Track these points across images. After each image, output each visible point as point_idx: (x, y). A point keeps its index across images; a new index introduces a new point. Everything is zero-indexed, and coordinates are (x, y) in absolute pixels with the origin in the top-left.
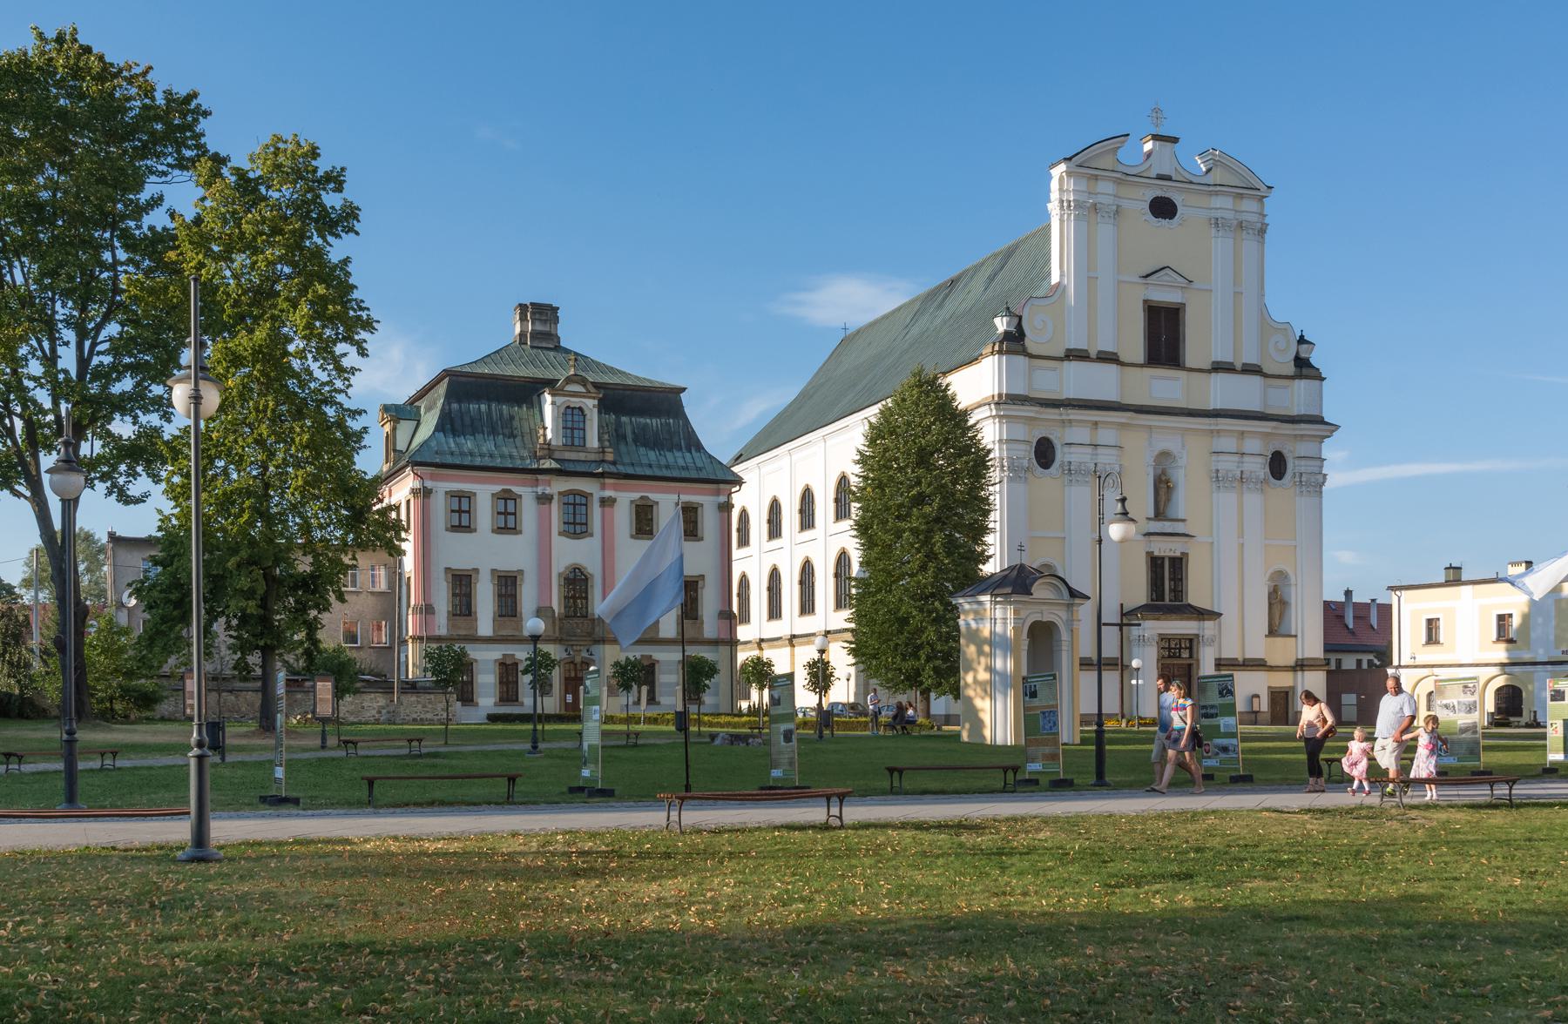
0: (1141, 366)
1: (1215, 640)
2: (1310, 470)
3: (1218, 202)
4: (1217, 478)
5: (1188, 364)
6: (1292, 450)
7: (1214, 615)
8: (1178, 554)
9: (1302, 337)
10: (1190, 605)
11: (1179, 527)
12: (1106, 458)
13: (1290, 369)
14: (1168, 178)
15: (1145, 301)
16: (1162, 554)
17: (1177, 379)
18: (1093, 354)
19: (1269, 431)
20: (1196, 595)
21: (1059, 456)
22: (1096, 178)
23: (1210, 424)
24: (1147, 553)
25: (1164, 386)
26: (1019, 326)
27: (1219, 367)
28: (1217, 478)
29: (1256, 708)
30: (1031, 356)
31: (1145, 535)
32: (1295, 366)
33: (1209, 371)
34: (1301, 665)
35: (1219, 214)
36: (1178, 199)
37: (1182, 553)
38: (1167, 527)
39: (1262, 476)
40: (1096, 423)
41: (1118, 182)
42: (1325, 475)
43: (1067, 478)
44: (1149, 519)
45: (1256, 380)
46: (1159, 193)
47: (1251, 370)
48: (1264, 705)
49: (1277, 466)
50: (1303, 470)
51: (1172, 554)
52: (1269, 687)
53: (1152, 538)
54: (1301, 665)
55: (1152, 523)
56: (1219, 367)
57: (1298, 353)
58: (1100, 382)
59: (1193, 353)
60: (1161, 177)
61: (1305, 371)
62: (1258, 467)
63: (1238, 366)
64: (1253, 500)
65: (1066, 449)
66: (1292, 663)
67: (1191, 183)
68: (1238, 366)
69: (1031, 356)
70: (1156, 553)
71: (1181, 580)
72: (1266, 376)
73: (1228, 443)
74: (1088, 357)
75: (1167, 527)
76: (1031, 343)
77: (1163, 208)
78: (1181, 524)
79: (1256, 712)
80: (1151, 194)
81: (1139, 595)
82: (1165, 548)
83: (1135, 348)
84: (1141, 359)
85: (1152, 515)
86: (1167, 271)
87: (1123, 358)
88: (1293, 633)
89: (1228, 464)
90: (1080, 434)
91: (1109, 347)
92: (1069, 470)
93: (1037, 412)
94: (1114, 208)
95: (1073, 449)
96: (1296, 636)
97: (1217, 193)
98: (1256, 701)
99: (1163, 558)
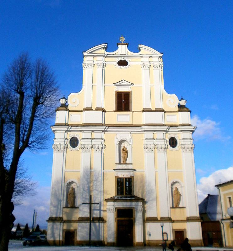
0: (114, 111)
3: (142, 59)
6: (178, 136)
8: (129, 176)
11: (130, 167)
14: (125, 55)
16: (123, 177)
17: (128, 115)
18: (94, 109)
19: (166, 130)
20: (137, 192)
22: (95, 56)
25: (124, 117)
27: (145, 110)
28: (146, 148)
29: (165, 238)
30: (69, 111)
31: (114, 170)
32: (178, 108)
34: (189, 220)
35: (142, 63)
37: (131, 176)
38: (124, 166)
39: (163, 146)
40: (93, 131)
43: (81, 150)
45: (160, 113)
46: (121, 59)
47: (157, 110)
48: (171, 237)
49: (173, 142)
50: (183, 143)
51: (127, 177)
53: (116, 171)
54: (189, 220)
56: (145, 110)
57: (179, 103)
58: (96, 117)
60: (121, 54)
61: (181, 109)
63: (153, 109)
64: (160, 156)
65: (81, 140)
66: (185, 219)
68: (153, 109)
70: (120, 176)
73: (150, 135)
74: (92, 109)
75: (124, 166)
76: (70, 108)
77: (123, 63)
79: (166, 240)
82: (124, 175)
85: (118, 163)
86: (124, 81)
89: (151, 143)
92: (83, 147)
94: (103, 64)
99: (123, 178)
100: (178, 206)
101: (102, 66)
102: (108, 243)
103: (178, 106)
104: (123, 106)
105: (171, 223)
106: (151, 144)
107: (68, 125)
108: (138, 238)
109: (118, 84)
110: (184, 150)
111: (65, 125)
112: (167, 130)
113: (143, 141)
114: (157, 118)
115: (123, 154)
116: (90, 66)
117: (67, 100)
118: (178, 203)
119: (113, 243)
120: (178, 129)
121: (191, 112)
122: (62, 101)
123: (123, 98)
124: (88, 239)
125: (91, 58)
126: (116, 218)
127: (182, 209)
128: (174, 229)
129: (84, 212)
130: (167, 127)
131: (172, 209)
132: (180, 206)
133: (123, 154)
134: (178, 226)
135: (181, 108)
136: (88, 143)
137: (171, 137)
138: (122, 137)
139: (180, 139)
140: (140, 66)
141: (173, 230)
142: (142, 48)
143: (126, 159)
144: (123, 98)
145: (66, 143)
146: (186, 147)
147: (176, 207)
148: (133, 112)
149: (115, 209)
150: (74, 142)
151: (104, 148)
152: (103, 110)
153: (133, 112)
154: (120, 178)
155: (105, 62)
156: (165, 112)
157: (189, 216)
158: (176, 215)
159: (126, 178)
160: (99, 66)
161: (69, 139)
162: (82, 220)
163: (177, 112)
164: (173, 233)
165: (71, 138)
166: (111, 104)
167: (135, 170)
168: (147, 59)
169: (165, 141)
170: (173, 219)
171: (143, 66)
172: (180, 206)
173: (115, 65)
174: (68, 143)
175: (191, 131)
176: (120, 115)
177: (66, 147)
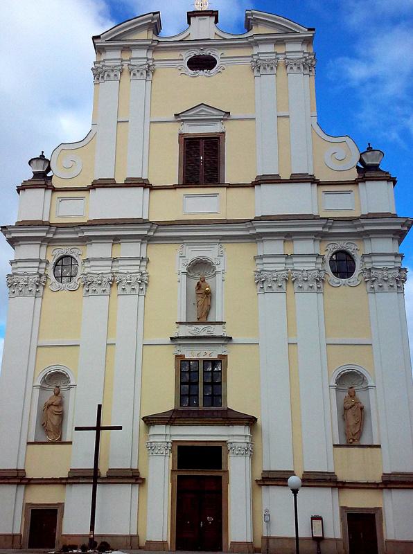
0: (174, 187)
1: (252, 453)
2: (381, 265)
3: (256, 50)
4: (261, 281)
6: (358, 250)
7: (251, 422)
8: (215, 356)
9: (370, 149)
10: (229, 409)
11: (217, 331)
12: (122, 267)
13: (354, 175)
17: (215, 195)
19: (320, 229)
20: (235, 400)
21: (80, 271)
23: (248, 230)
24: (176, 356)
29: (318, 534)
30: (54, 190)
31: (171, 338)
33: (253, 185)
36: (217, 54)
38: (202, 330)
42: (400, 270)
44: (180, 323)
46: (197, 53)
48: (335, 529)
52: (343, 509)
55: (182, 327)
57: (361, 161)
64: (308, 303)
65: (86, 264)
69: (54, 190)
71: (220, 383)
72: (319, 184)
73: (276, 247)
75: (202, 330)
76: (56, 183)
77: (202, 63)
80: (187, 55)
81: (167, 401)
87: (153, 183)
88: (375, 444)
89: (278, 266)
91: (136, 174)
94: (146, 66)
95: (92, 263)
96: (379, 446)
97: (257, 43)
98: (317, 523)
99: (197, 361)
100: (354, 443)
101: (145, 73)
102: (149, 542)
103: (357, 167)
104: (202, 173)
105: (336, 491)
106: (277, 269)
107: (50, 225)
108: (238, 528)
109: (191, 116)
110: (376, 285)
111: (42, 224)
112: (327, 230)
113: (258, 261)
114: (299, 200)
115: (203, 297)
116: (112, 75)
117: (49, 162)
118: (359, 434)
119: (164, 543)
120: (355, 227)
121: (395, 183)
123: (202, 151)
124: (88, 532)
125: (116, 55)
126: (172, 471)
127: (369, 449)
128: (345, 508)
129: (79, 454)
130: (324, 222)
131: (338, 449)
132: (364, 441)
133: (203, 297)
134: (360, 500)
135: (367, 172)
136: (104, 268)
137: (335, 250)
138: (194, 252)
139: (364, 256)
140: (248, 67)
141: (343, 509)
142: (255, 19)
143: (207, 313)
144: (202, 151)
145: (42, 271)
146: (380, 277)
147: (349, 445)
148: (229, 186)
149: (170, 444)
151: (143, 283)
152: (144, 184)
153: (229, 186)
154: (189, 361)
155: (154, 60)
156: (319, 184)
157: (388, 471)
158: (353, 466)
159: (206, 362)
160: (136, 73)
161: (52, 261)
162: (76, 478)
163: (356, 182)
164: (341, 519)
165: (56, 258)
166: (169, 168)
167: (231, 338)
168: (270, 48)
169: (320, 261)
170: (342, 476)
171: (257, 66)
172: (364, 441)
173: (179, 68)
174: (50, 273)
175: (396, 232)
176: (188, 196)
177: (41, 283)
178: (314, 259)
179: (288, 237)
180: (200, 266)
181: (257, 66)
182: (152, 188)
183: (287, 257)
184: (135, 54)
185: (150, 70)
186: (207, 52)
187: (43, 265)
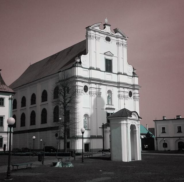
0: (105, 72)
4: (119, 96)
5: (113, 72)
6: (133, 92)
11: (112, 107)
13: (132, 75)
15: (105, 58)
16: (109, 112)
26: (80, 61)
27: (119, 74)
36: (111, 37)
41: (100, 33)
49: (130, 94)
59: (115, 69)
62: (127, 94)
67: (113, 35)
70: (108, 112)
73: (121, 89)
75: (110, 107)
77: (108, 39)
78: (113, 106)
80: (106, 36)
83: (103, 68)
84: (104, 70)
86: (109, 52)
90: (93, 85)
93: (84, 80)
122: (78, 61)
150: (86, 89)
163: (133, 77)
168: (120, 39)
176: (107, 74)
178: (127, 93)
179: (124, 88)
180: (109, 92)
181: (118, 43)
182: (101, 71)
183: (124, 92)
184: (97, 33)
185: (99, 38)
186: (109, 36)
187: (82, 87)
